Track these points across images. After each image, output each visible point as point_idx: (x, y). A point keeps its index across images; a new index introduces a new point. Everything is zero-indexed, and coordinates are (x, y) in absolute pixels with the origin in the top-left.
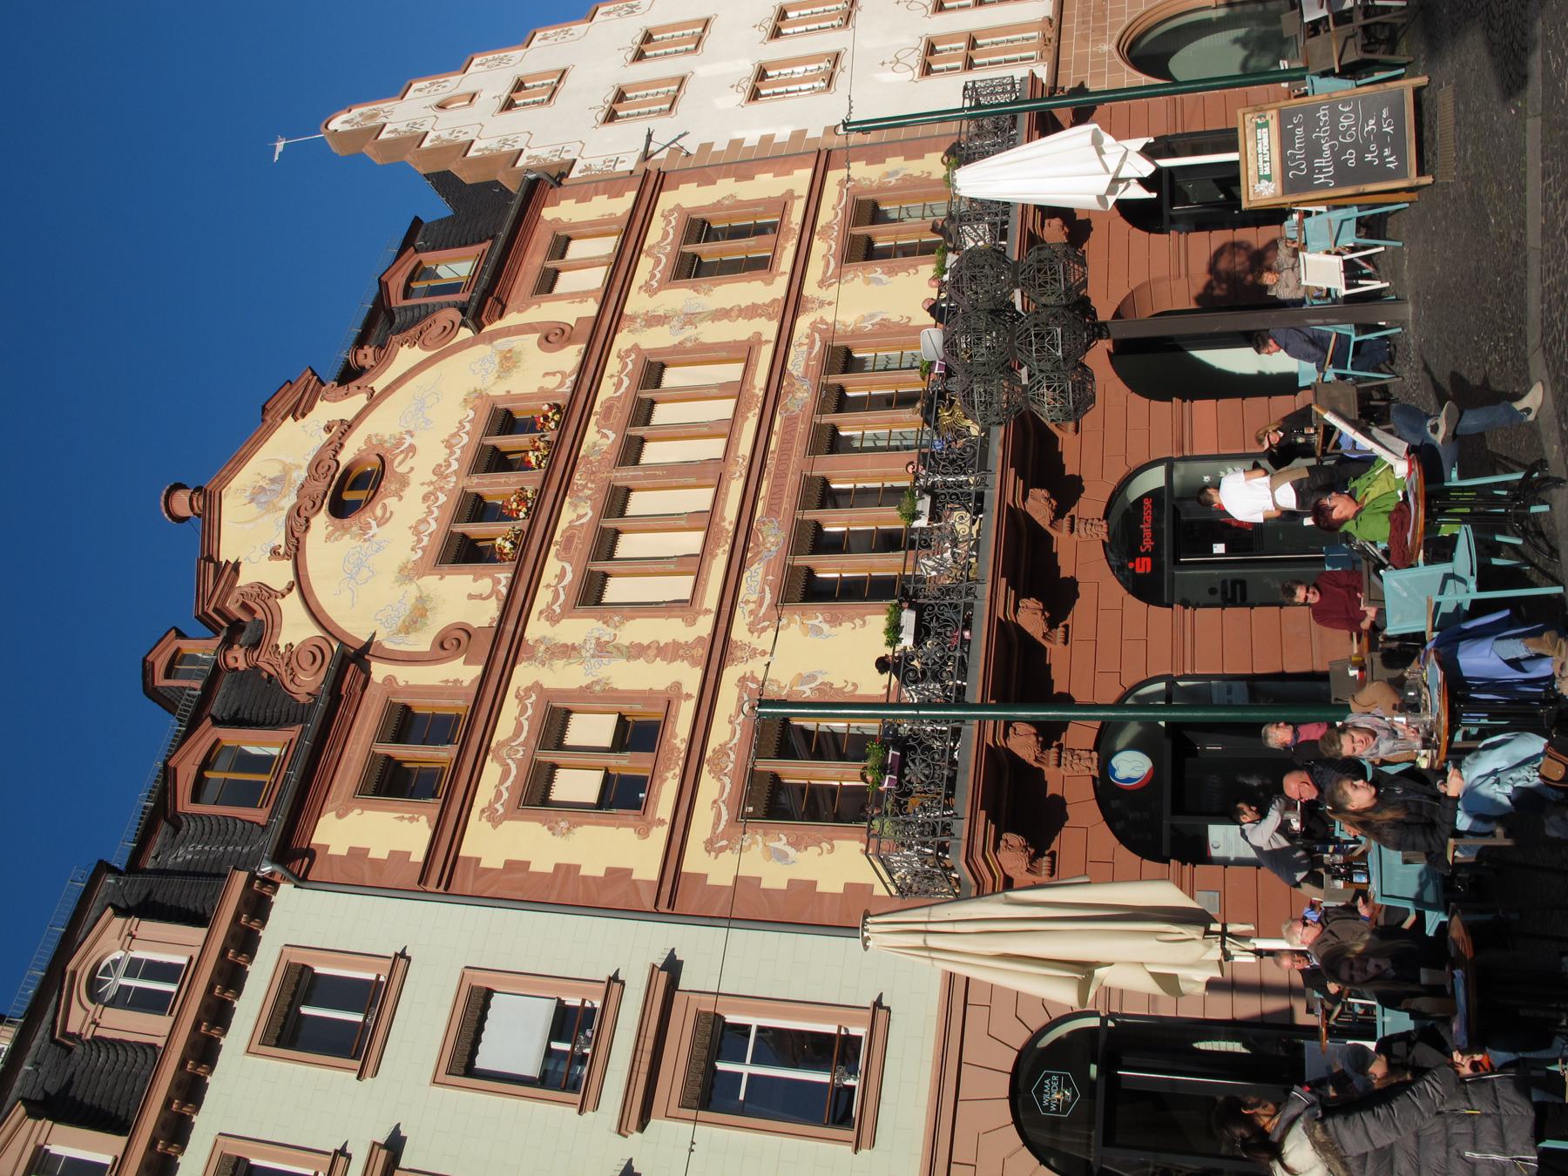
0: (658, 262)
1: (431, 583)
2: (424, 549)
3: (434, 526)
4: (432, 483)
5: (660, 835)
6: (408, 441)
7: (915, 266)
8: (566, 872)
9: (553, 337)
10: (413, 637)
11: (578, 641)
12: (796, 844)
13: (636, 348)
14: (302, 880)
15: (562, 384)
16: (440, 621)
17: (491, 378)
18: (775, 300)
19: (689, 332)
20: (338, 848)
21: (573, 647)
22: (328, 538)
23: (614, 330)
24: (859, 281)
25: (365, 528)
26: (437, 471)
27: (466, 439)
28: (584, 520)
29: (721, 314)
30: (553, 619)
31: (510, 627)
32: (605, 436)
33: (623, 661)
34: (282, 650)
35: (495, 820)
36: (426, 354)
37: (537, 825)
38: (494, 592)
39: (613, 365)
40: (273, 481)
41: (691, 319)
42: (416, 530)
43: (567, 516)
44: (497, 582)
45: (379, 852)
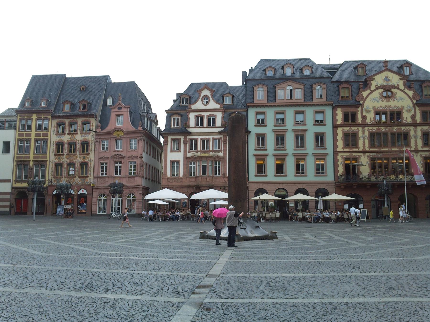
0: (427, 129)
1: (373, 111)
2: (378, 109)
3: (381, 109)
4: (388, 106)
5: (342, 150)
6: (395, 99)
7: (423, 167)
8: (337, 140)
9: (413, 117)
10: (365, 112)
11: (365, 134)
12: (342, 165)
13: (411, 130)
14: (333, 109)
15: (404, 120)
16: (367, 115)
17: (406, 109)
18: (418, 148)
19: (413, 137)
20: (337, 112)
21: (364, 134)
22: (379, 93)
23: (414, 126)
24: (421, 160)
25: (381, 98)
26: (390, 106)
27: (395, 109)
28: (382, 130)
29: (416, 141)
30: (368, 130)
31: (366, 125)
32: (395, 129)
33: (363, 141)
34: (362, 93)
35: (342, 131)
36: (411, 96)
37: (342, 136)
38: (371, 121)
39: (407, 128)
40: (389, 79)
41: (415, 137)
42: (381, 106)
43: (383, 128)
44: (373, 121)
45: (337, 117)
